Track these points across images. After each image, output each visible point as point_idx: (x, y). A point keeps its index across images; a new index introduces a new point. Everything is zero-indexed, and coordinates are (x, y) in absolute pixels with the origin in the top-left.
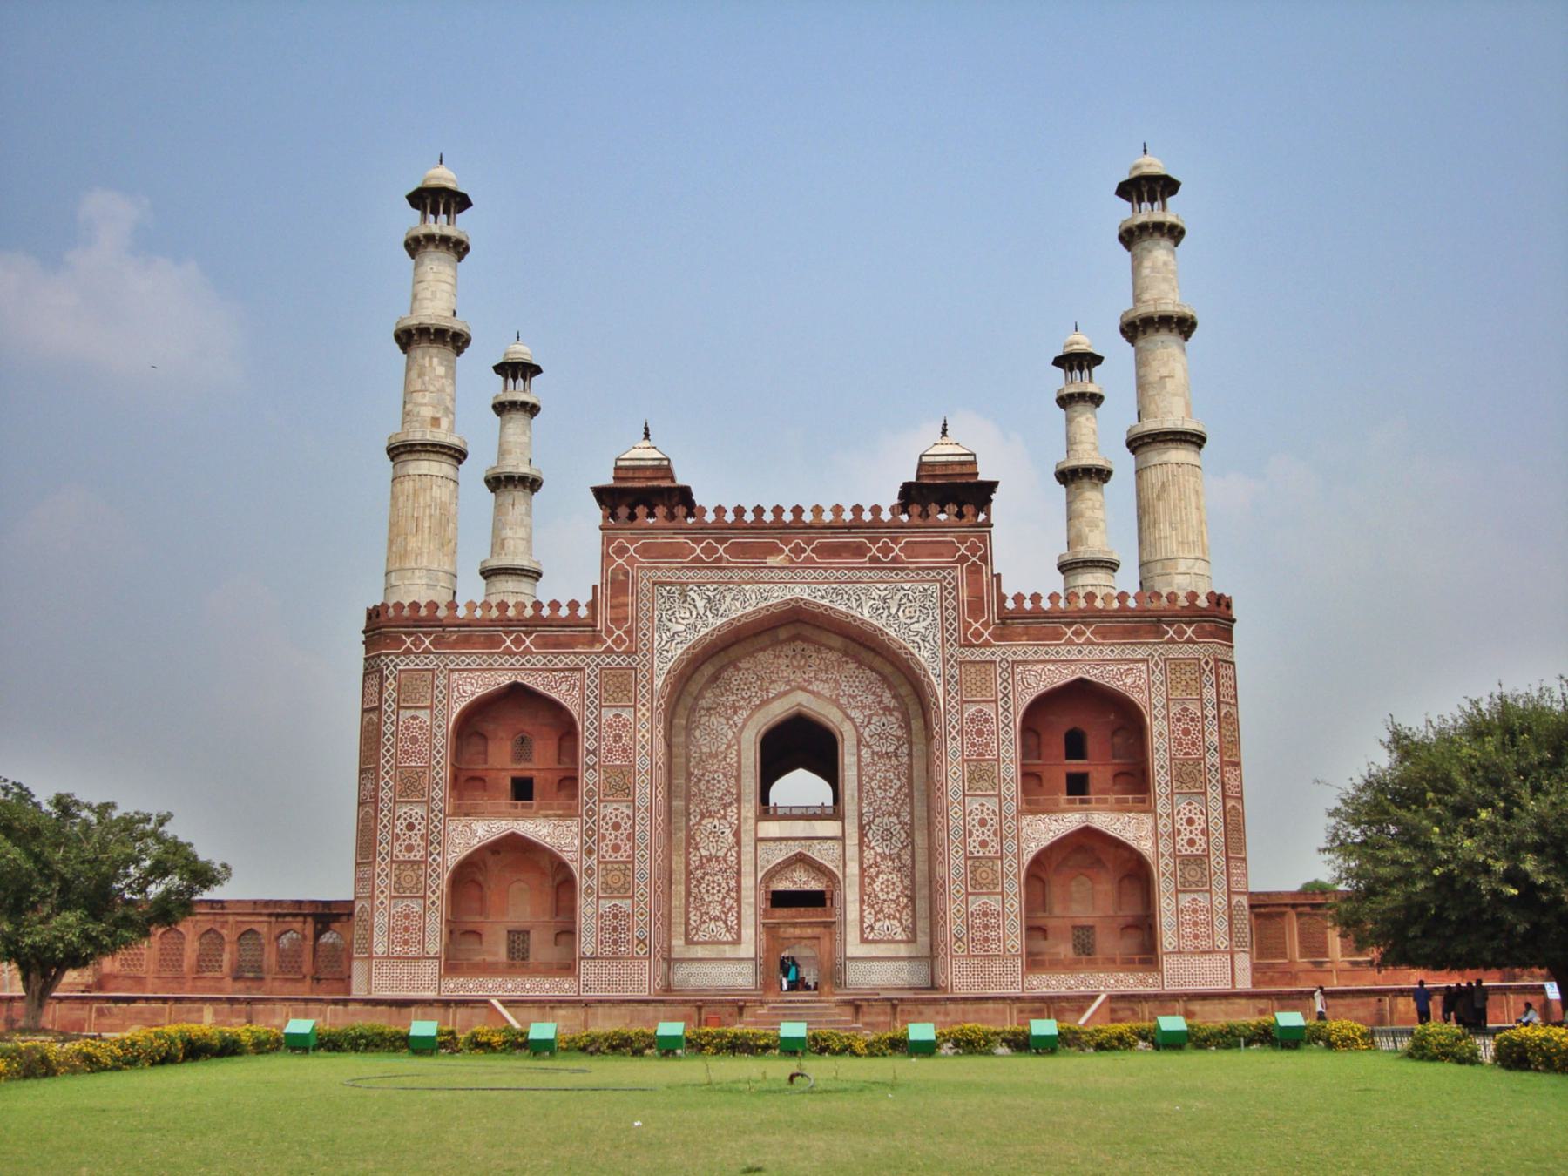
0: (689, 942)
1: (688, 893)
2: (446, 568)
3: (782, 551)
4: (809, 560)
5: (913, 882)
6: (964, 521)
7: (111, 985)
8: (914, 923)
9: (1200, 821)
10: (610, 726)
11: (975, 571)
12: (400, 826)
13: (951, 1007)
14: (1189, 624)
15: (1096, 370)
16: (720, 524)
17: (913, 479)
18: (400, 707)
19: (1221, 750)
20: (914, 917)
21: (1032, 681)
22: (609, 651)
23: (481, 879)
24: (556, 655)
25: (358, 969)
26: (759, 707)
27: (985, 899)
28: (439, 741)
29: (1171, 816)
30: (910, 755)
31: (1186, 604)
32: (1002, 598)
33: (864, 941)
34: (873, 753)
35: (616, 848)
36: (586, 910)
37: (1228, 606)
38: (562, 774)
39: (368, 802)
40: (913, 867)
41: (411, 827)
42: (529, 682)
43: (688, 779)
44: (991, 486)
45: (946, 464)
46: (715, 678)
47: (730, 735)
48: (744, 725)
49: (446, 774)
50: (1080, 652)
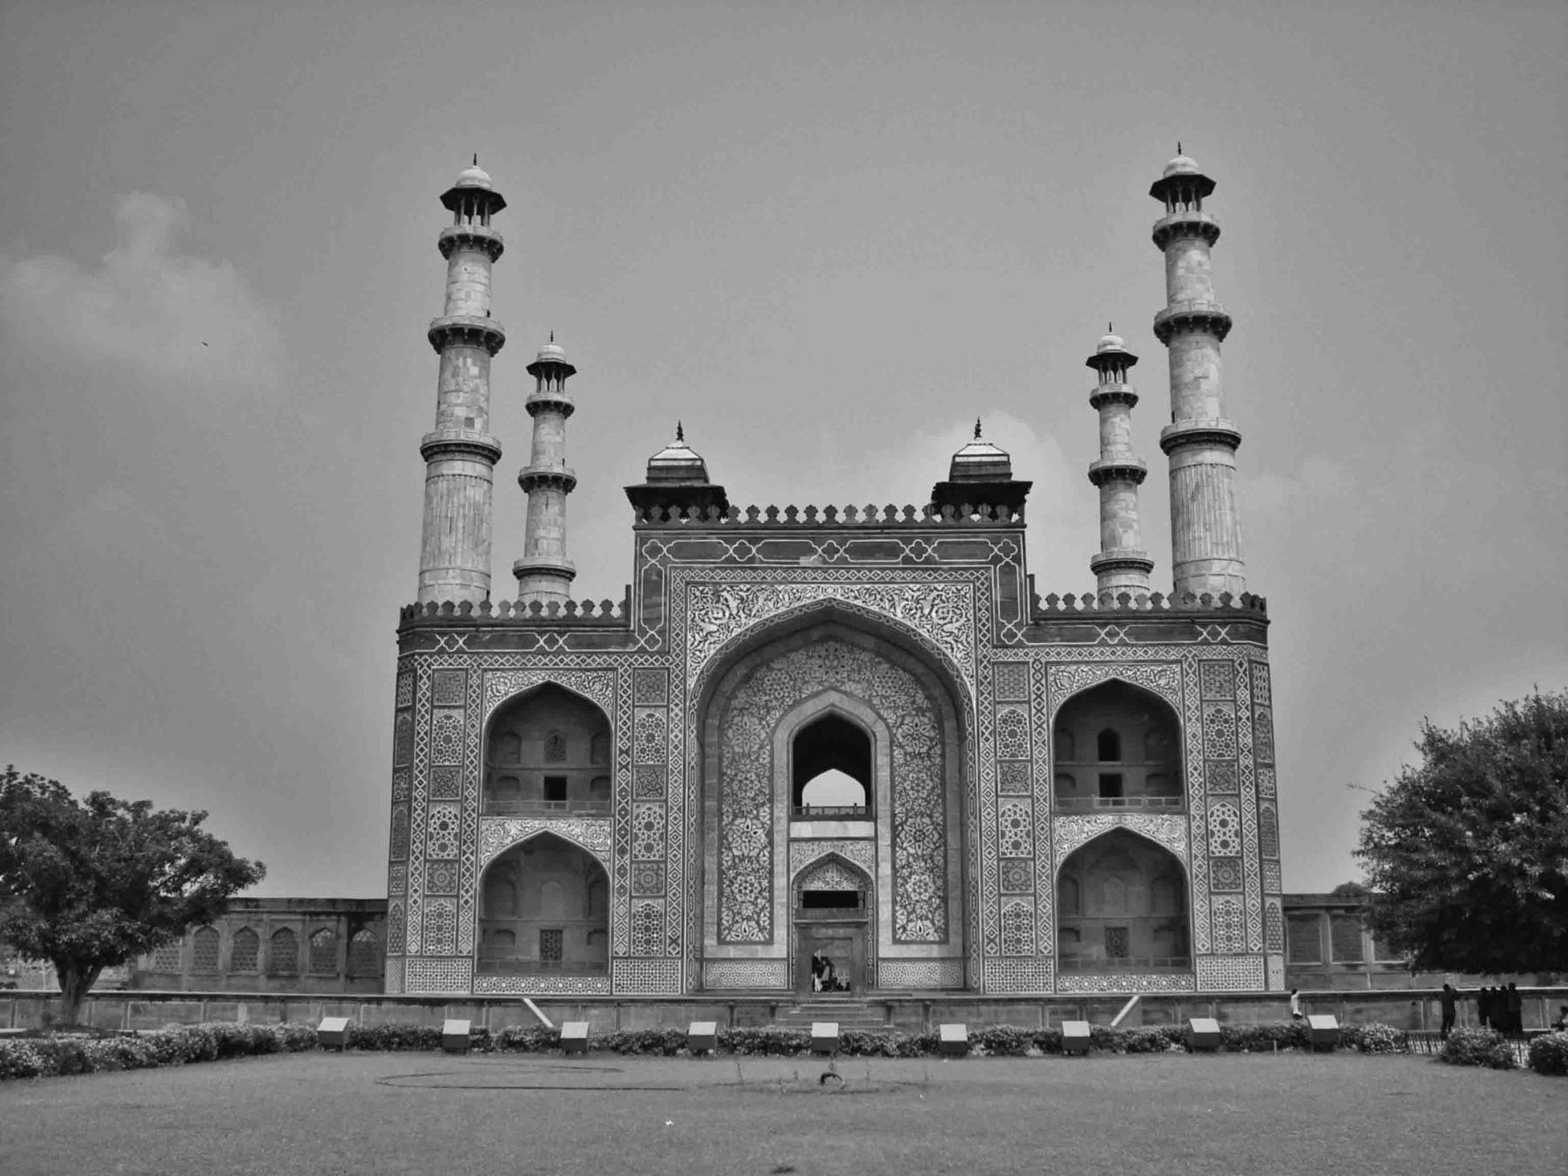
0: (721, 941)
1: (721, 893)
2: (481, 568)
3: (815, 552)
4: (843, 560)
6: (998, 522)
7: (147, 982)
8: (946, 924)
9: (1233, 823)
10: (643, 726)
11: (1008, 571)
12: (434, 825)
13: (984, 1008)
14: (1223, 625)
15: (1130, 371)
16: (753, 523)
17: (946, 479)
18: (433, 707)
19: (1255, 752)
20: (946, 918)
21: (1066, 682)
22: (642, 651)
23: (512, 877)
24: (589, 655)
25: (391, 968)
26: (791, 707)
27: (1017, 900)
28: (473, 741)
29: (1204, 818)
30: (943, 756)
31: (1220, 605)
32: (1035, 599)
33: (896, 941)
35: (649, 848)
36: (618, 908)
37: (1263, 607)
38: (595, 774)
39: (402, 802)
41: (444, 826)
42: (562, 681)
43: (721, 780)
44: (1025, 487)
45: (980, 464)
46: (748, 678)
47: (763, 735)
48: (777, 726)
49: (479, 773)
50: (1113, 653)
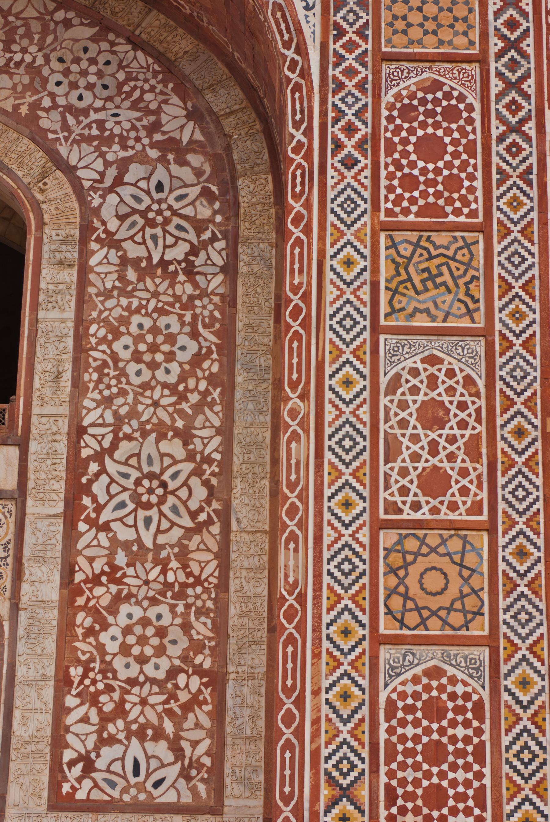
5: (220, 629)
34: (124, 261)
40: (223, 585)
